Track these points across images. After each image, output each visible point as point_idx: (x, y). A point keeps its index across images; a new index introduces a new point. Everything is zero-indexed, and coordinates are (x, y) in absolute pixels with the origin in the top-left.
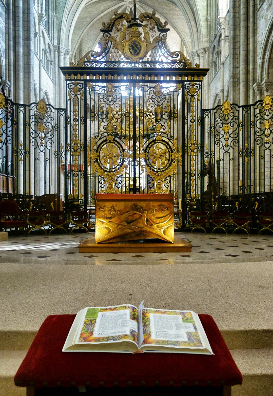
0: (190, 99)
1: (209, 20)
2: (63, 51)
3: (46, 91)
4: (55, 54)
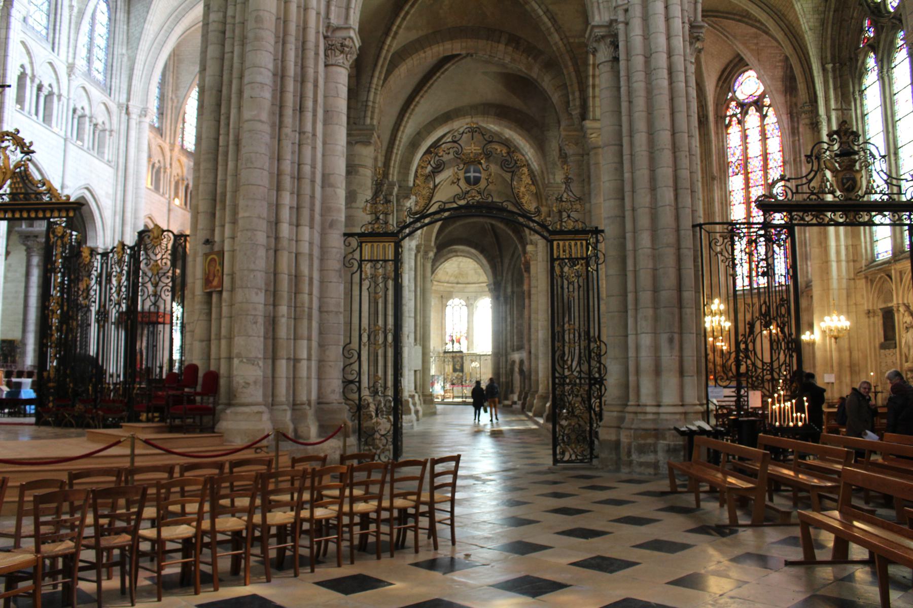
2: (135, 111)
4: (120, 117)
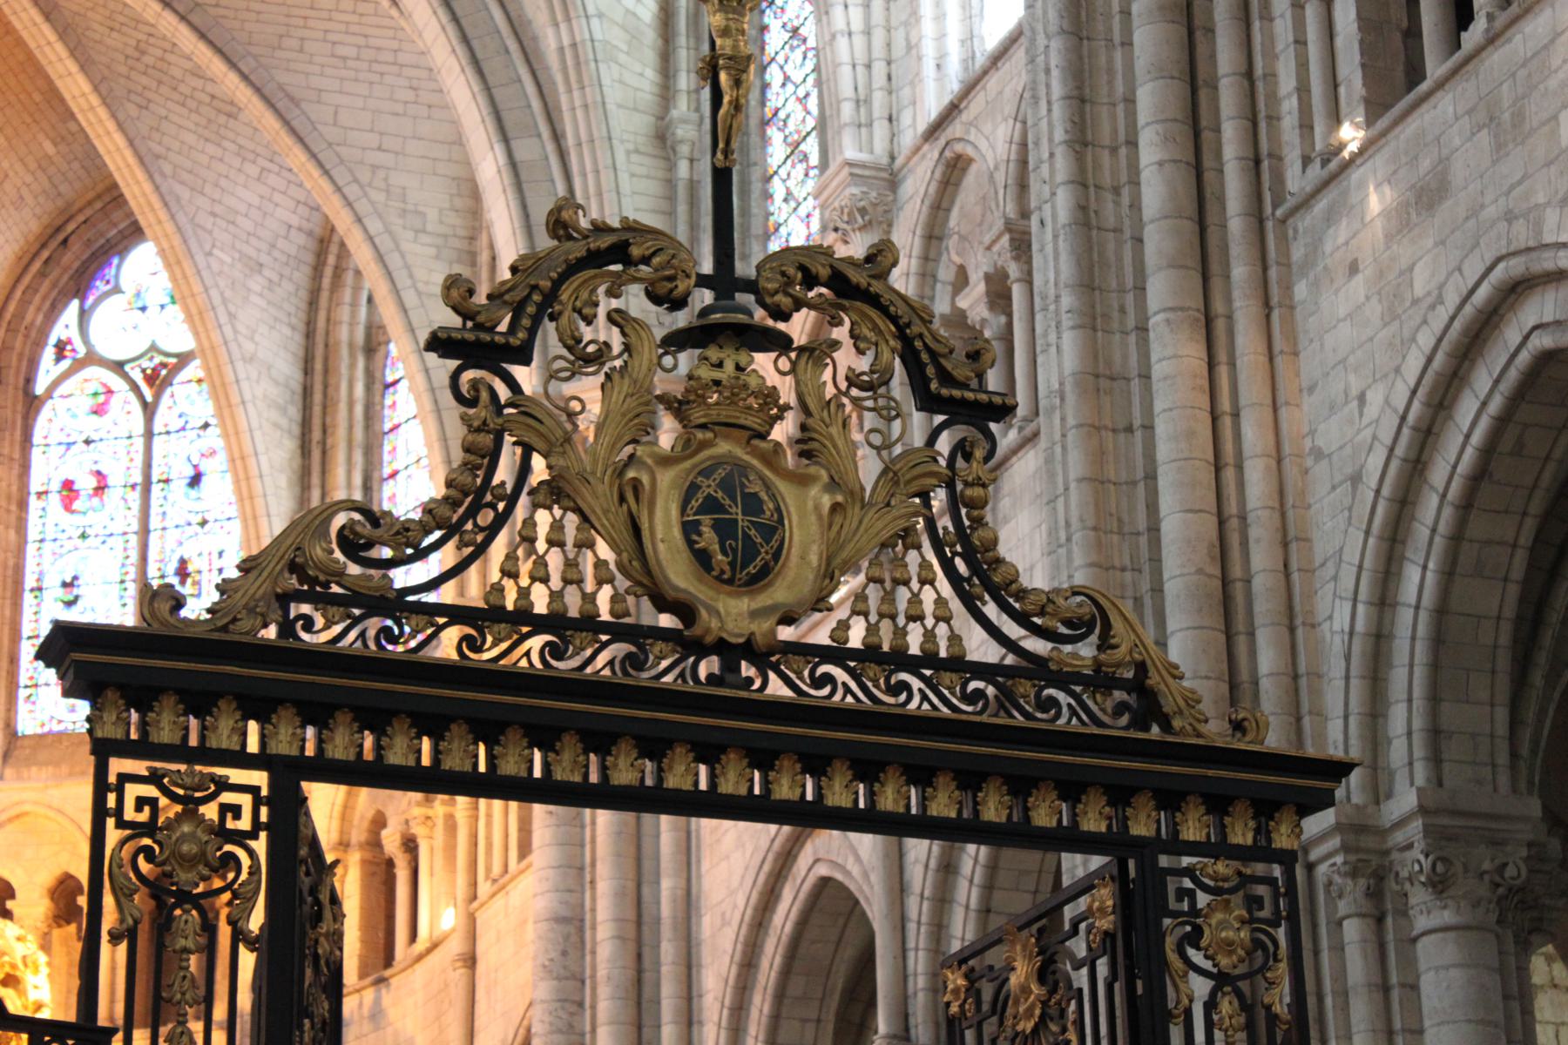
0: (1211, 1006)
1: (684, 150)
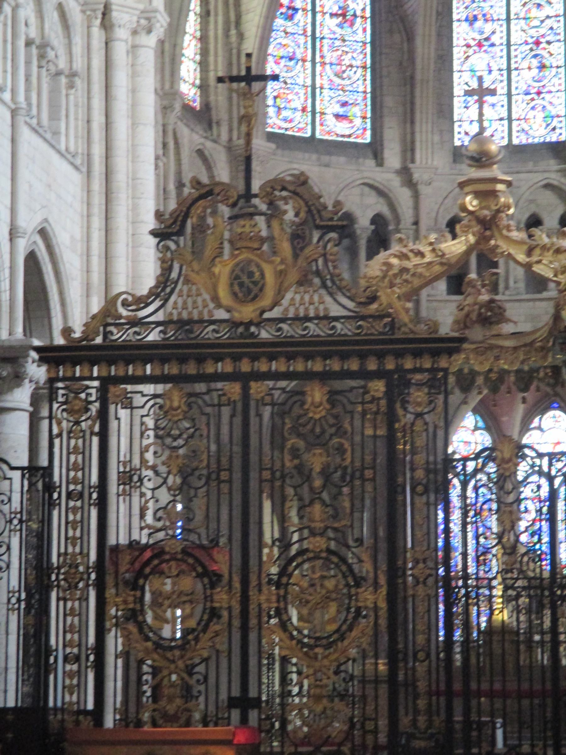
3: (46, 220)
4: (89, 36)
